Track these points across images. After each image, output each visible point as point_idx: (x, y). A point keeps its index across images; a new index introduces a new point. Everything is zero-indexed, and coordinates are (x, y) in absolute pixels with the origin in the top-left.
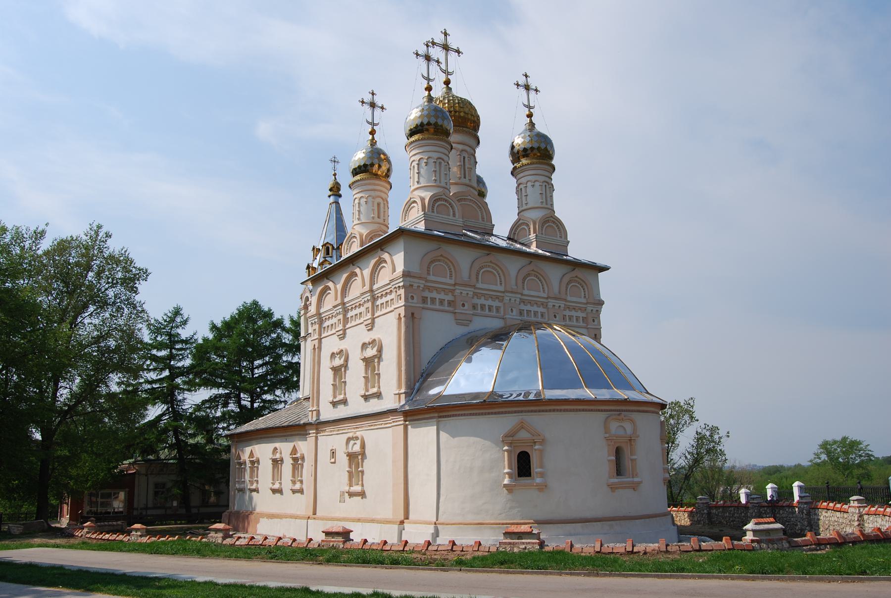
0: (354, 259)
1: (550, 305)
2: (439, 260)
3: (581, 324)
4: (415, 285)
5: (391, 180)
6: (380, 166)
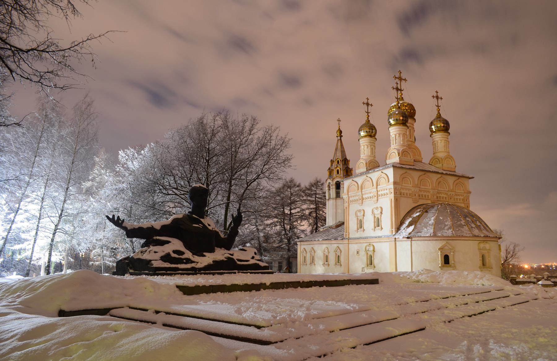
3: (461, 201)
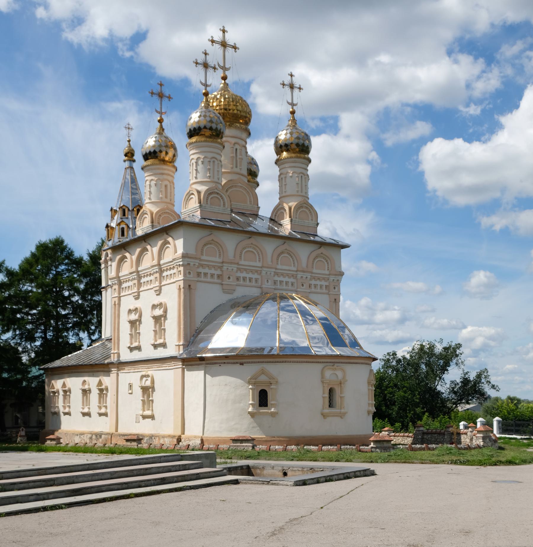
0: (146, 238)
1: (299, 276)
2: (211, 244)
3: (324, 291)
4: (192, 264)
5: (176, 164)
6: (167, 153)
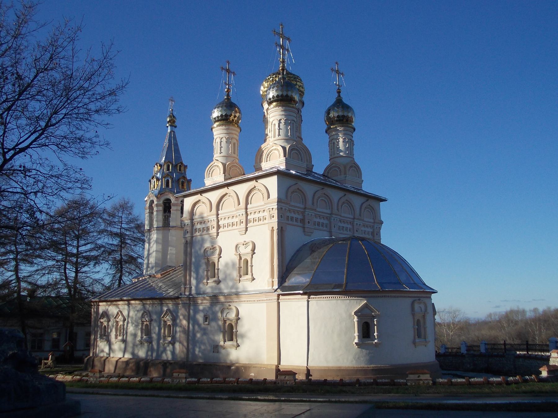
4: (284, 208)
